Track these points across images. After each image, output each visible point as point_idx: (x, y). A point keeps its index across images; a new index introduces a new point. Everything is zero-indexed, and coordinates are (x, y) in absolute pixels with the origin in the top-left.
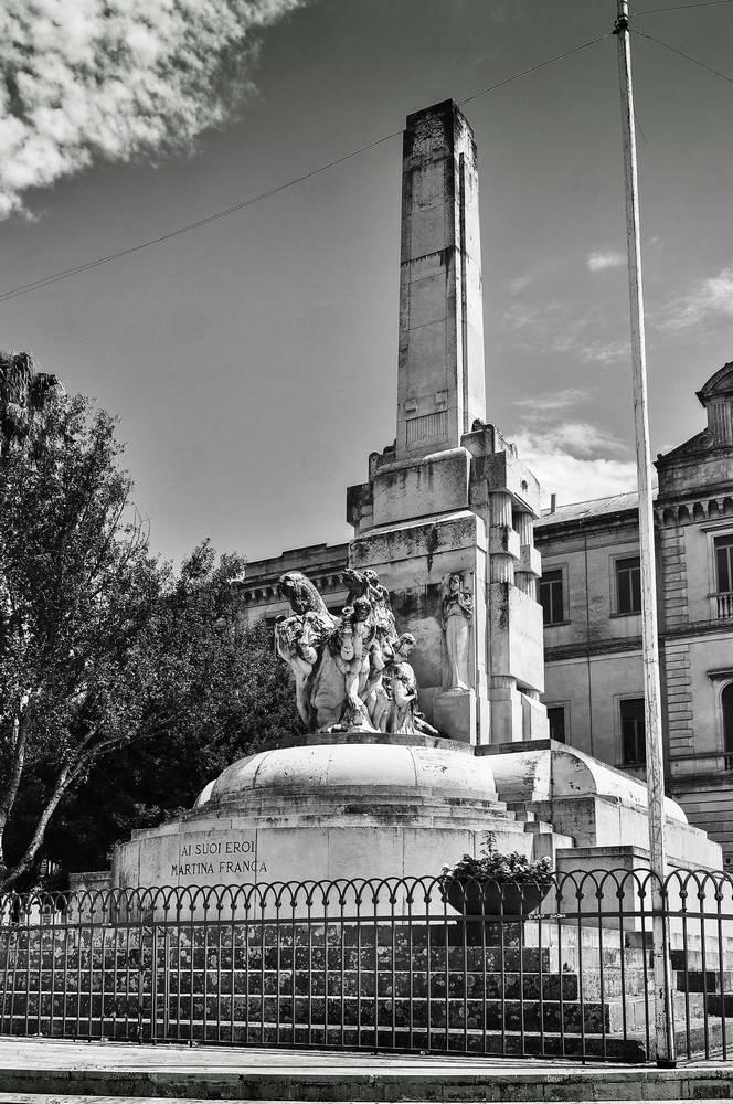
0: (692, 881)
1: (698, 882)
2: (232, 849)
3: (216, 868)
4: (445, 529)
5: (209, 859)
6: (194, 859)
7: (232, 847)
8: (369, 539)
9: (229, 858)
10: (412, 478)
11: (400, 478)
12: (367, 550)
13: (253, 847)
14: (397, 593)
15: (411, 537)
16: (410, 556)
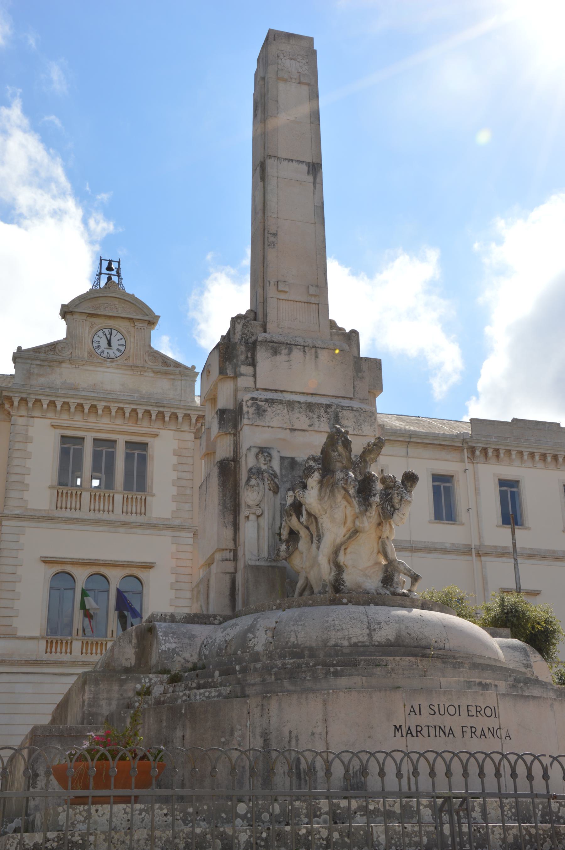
0: (389, 760)
1: (378, 762)
2: (473, 712)
3: (458, 732)
4: (346, 413)
5: (448, 722)
6: (425, 719)
7: (473, 709)
8: (266, 400)
9: (471, 722)
10: (297, 354)
11: (284, 351)
12: (265, 411)
13: (495, 713)
14: (299, 460)
15: (311, 411)
16: (311, 428)
